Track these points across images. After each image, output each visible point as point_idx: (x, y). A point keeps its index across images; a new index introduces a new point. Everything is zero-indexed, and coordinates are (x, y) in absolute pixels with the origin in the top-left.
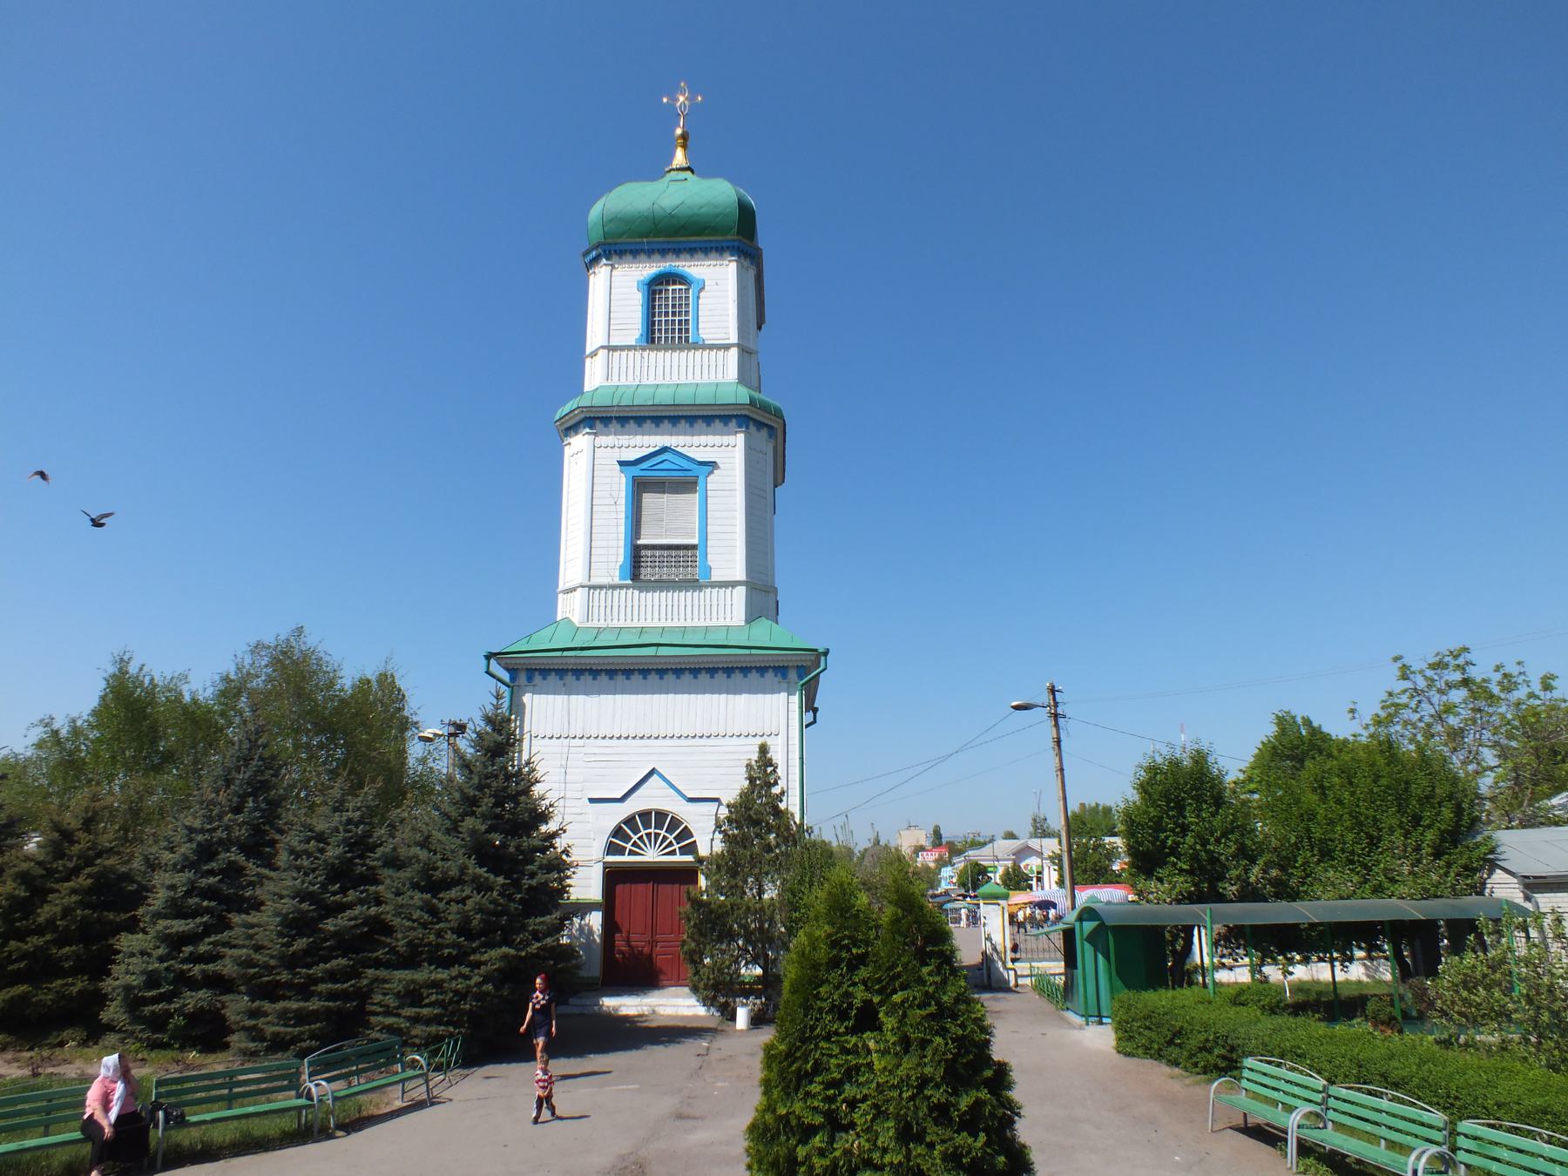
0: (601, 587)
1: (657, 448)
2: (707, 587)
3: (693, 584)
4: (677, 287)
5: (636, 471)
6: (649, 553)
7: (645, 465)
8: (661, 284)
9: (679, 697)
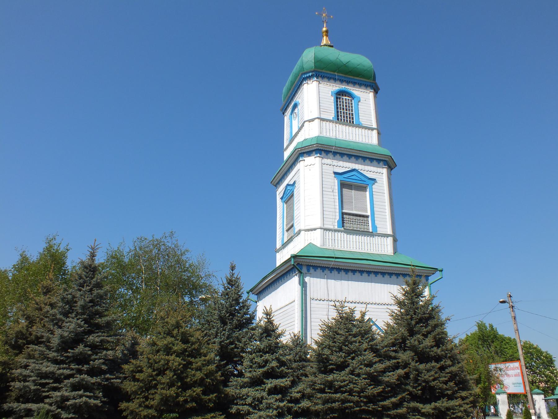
0: (329, 230)
1: (350, 169)
2: (376, 236)
3: (371, 234)
5: (341, 178)
6: (348, 216)
7: (346, 176)
8: (340, 95)
9: (377, 284)
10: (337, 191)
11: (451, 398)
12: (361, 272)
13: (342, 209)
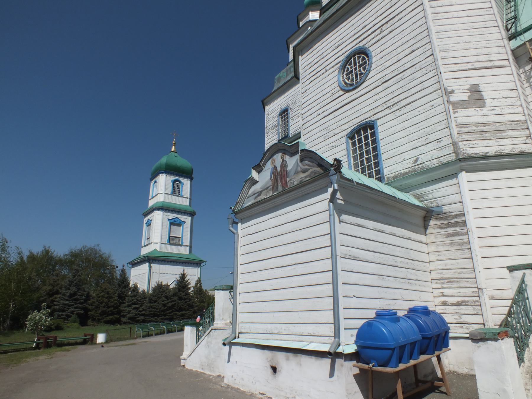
4: (178, 183)
6: (172, 238)
7: (173, 220)
8: (175, 181)
10: (168, 227)
11: (186, 311)
12: (174, 262)
13: (170, 234)
